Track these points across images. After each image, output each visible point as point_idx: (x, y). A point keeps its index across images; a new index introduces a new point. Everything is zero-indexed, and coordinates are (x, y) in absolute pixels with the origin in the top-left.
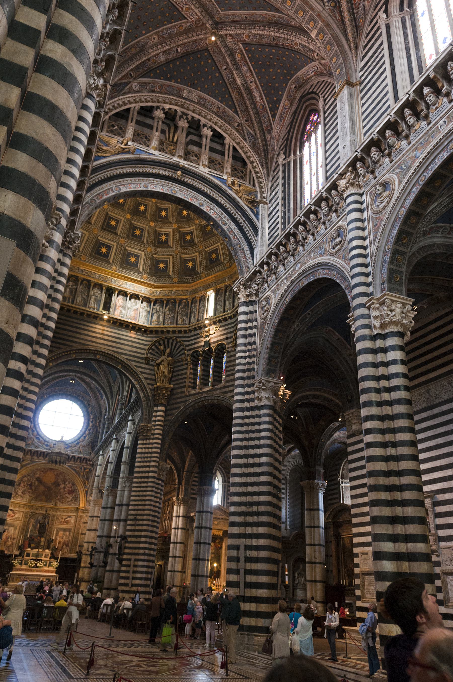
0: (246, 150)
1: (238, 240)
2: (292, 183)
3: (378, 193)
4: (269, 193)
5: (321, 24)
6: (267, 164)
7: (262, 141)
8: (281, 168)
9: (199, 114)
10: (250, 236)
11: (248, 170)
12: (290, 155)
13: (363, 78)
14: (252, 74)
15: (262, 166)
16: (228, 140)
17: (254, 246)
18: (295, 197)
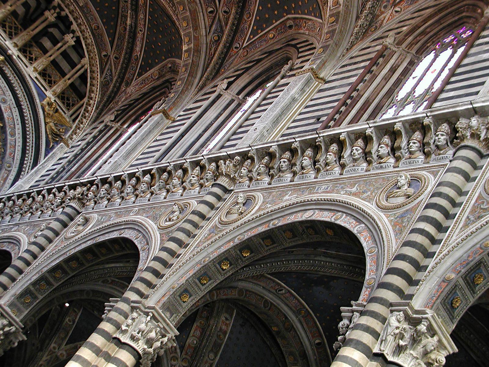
0: (95, 82)
1: (13, 159)
2: (95, 148)
3: (78, 223)
4: (79, 139)
5: (192, 45)
6: (102, 110)
7: (114, 87)
8: (101, 126)
9: (76, 19)
10: (26, 164)
11: (82, 102)
12: (118, 122)
13: (179, 118)
14: (145, 25)
15: (97, 108)
16: (85, 60)
17: (21, 176)
18: (85, 162)
